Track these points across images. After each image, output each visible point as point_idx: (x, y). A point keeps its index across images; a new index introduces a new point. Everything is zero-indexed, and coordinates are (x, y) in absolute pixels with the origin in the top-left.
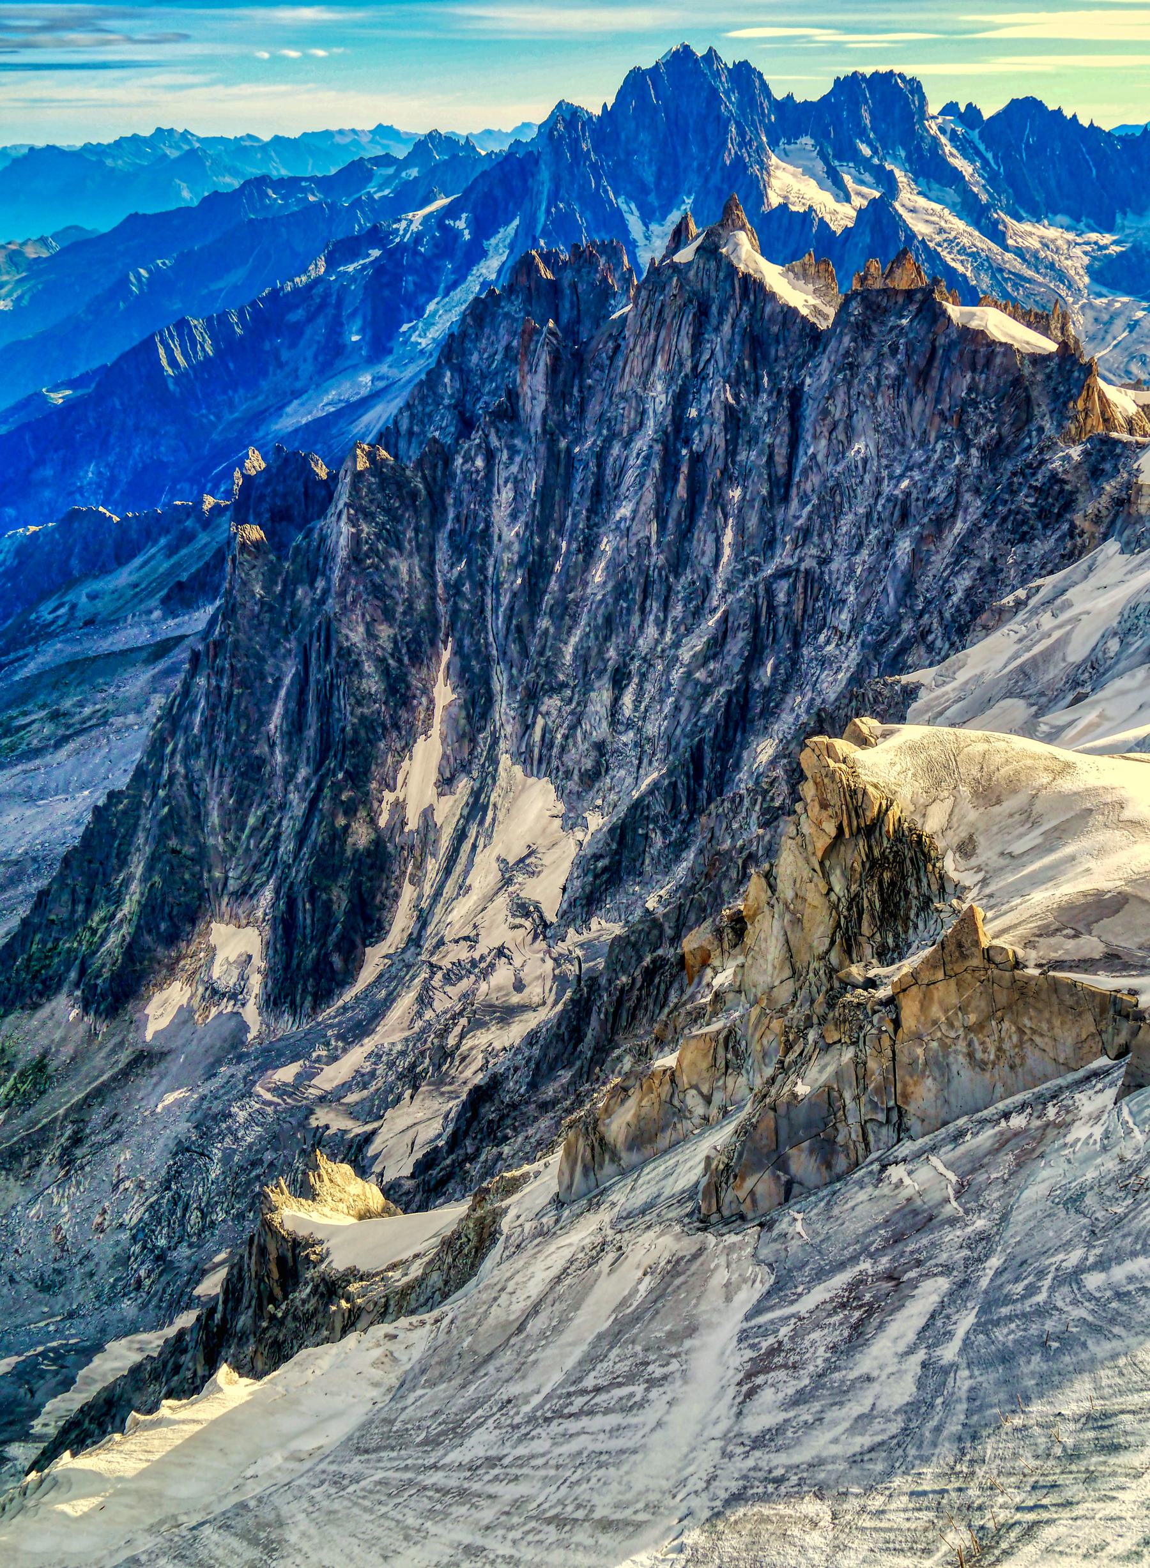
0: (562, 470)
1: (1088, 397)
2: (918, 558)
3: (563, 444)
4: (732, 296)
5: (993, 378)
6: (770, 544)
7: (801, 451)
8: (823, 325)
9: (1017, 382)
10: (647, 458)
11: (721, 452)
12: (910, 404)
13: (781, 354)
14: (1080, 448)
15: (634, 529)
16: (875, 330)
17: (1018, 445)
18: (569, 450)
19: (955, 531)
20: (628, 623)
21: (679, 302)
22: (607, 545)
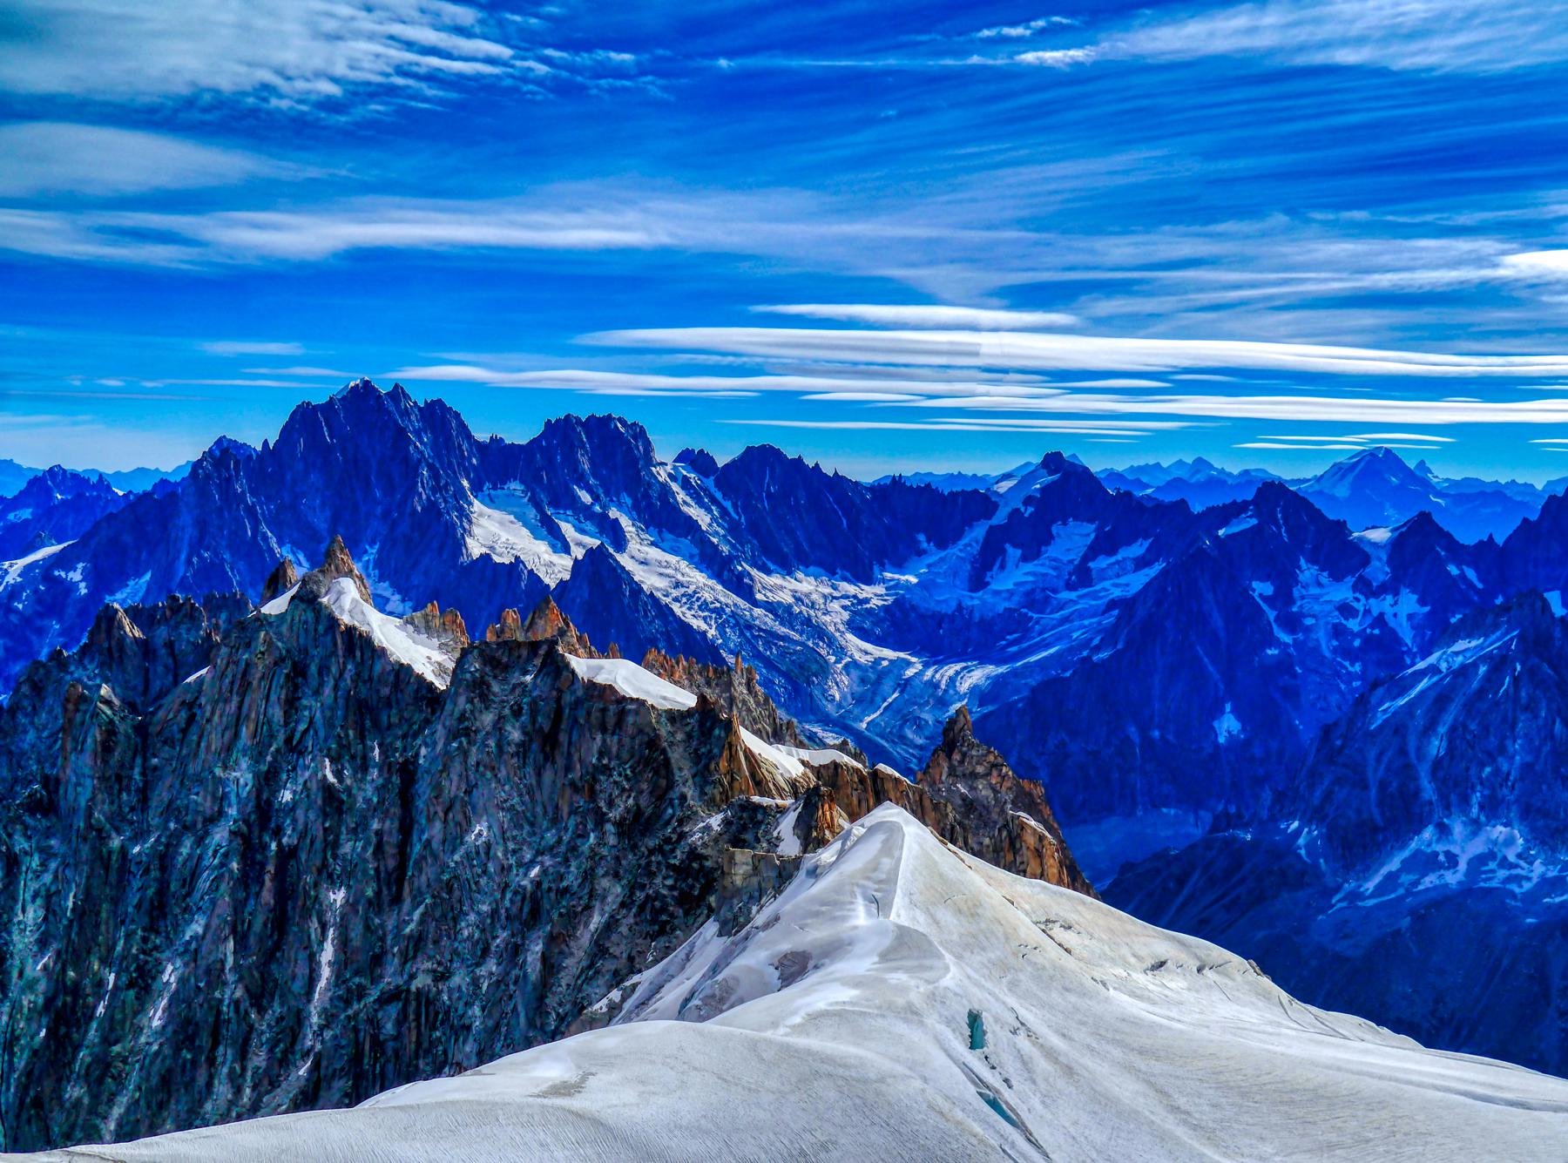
0: (113, 878)
1: (733, 757)
2: (550, 966)
3: (116, 842)
4: (334, 653)
5: (627, 741)
6: (378, 960)
7: (415, 838)
8: (441, 685)
9: (653, 742)
10: (226, 855)
11: (318, 845)
12: (539, 775)
13: (394, 720)
14: (720, 816)
15: (204, 950)
16: (496, 688)
17: (660, 817)
18: (123, 851)
19: (592, 927)
20: (193, 1080)
21: (269, 660)
22: (170, 975)
